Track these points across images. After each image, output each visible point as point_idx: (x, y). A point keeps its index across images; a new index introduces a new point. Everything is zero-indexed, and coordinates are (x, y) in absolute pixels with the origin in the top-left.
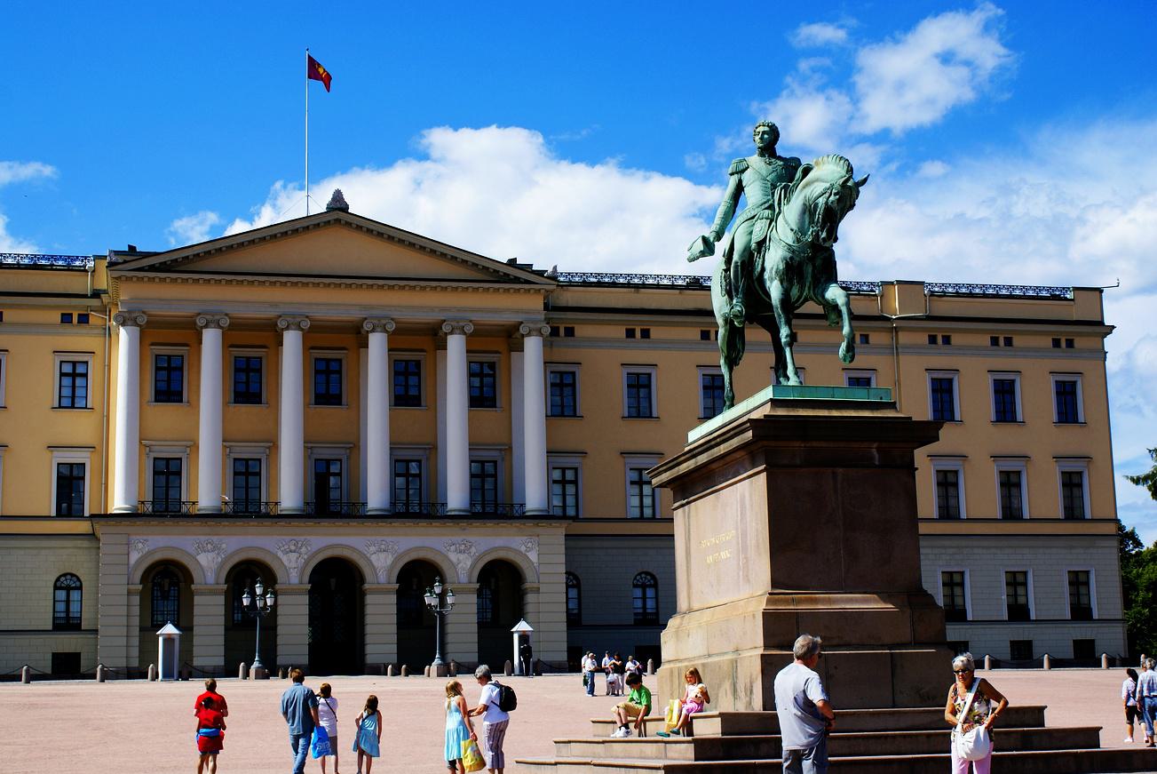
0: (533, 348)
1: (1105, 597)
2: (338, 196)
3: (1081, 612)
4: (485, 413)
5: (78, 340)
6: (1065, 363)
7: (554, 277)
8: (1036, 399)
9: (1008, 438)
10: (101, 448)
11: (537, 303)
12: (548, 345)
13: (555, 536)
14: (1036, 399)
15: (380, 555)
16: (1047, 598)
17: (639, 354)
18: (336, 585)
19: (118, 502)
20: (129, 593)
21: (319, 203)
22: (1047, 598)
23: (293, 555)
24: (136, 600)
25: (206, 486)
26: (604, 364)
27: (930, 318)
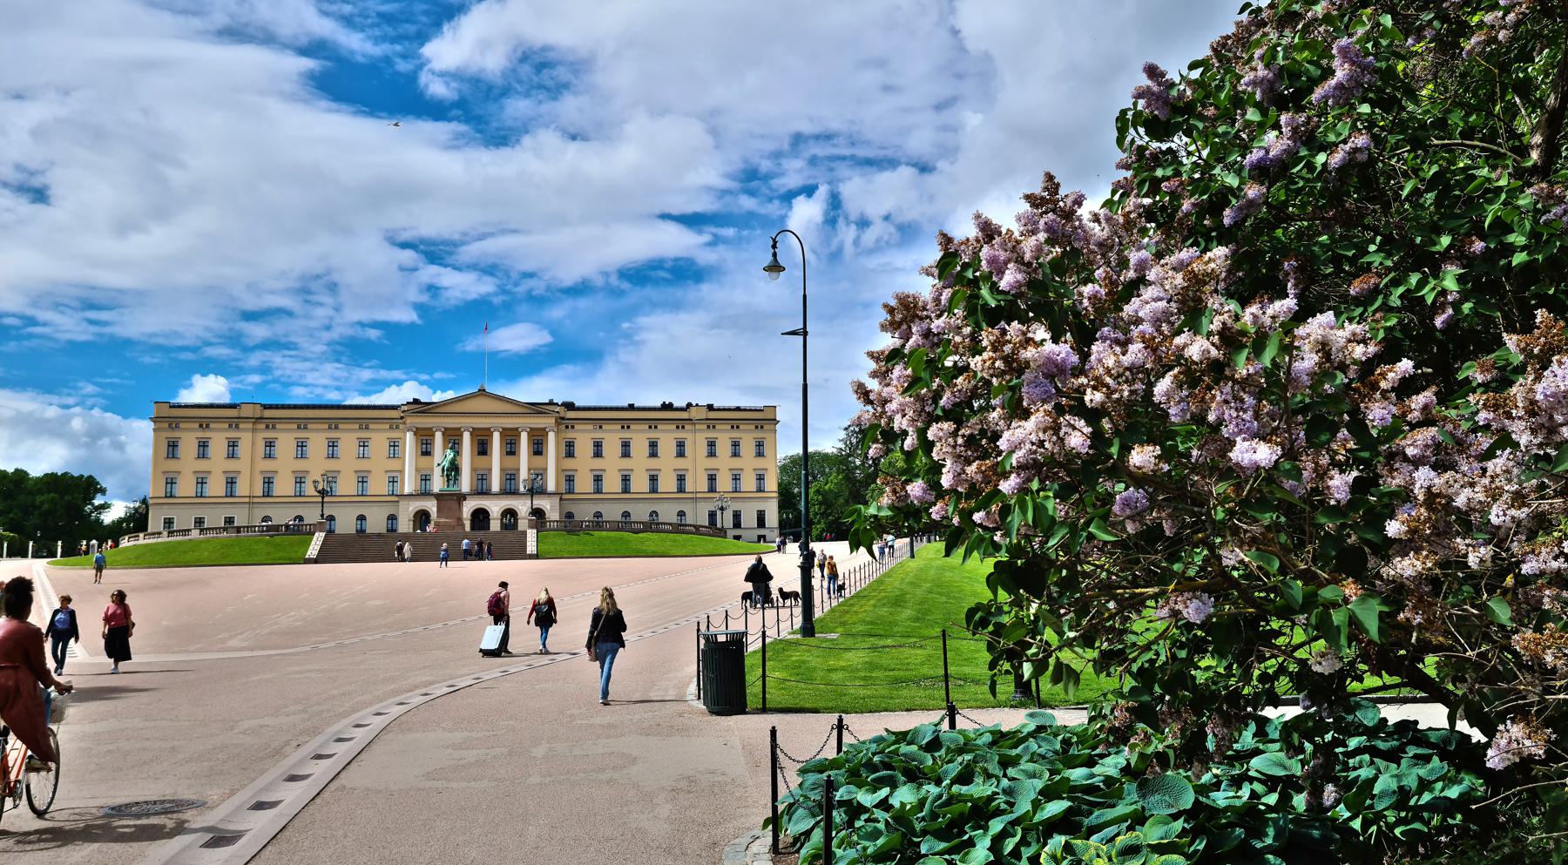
0: (551, 436)
1: (772, 519)
4: (538, 458)
5: (395, 434)
6: (759, 434)
7: (570, 406)
8: (748, 448)
10: (402, 472)
11: (553, 421)
12: (557, 433)
13: (556, 500)
14: (748, 448)
16: (749, 519)
17: (598, 435)
19: (407, 491)
22: (749, 519)
26: (584, 440)
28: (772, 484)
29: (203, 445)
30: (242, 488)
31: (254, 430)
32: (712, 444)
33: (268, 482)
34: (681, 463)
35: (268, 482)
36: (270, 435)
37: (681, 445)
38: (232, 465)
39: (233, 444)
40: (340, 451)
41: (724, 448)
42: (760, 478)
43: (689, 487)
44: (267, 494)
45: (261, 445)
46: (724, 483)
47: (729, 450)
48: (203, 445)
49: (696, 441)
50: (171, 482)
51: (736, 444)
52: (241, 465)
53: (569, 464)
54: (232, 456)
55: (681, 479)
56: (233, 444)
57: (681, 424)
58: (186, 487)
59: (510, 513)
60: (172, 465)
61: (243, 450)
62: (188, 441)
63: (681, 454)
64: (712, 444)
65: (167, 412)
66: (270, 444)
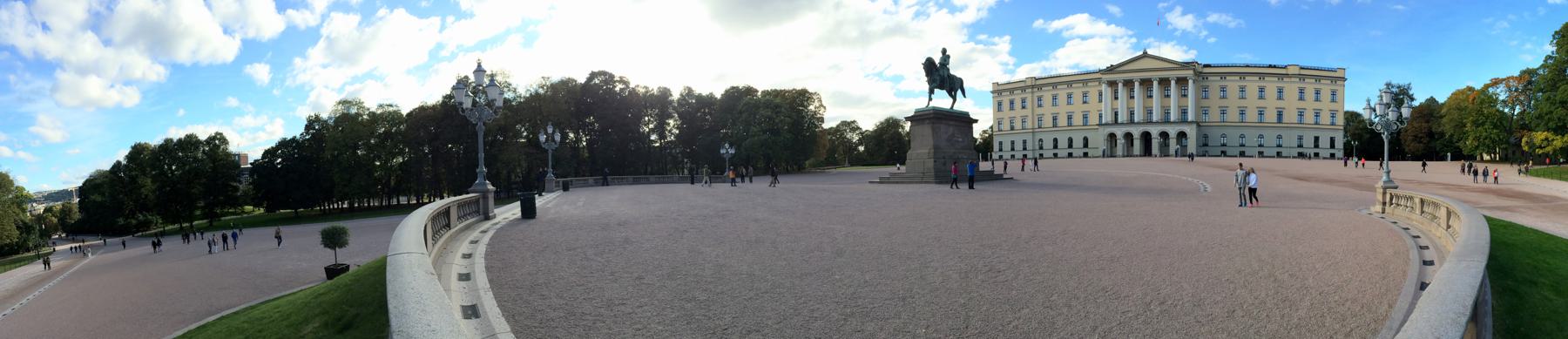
1: (1339, 144)
3: (1332, 146)
9: (1317, 105)
15: (1155, 131)
16: (1324, 143)
18: (1146, 137)
23: (1136, 132)
25: (1122, 118)
29: (1012, 103)
30: (1029, 125)
32: (1302, 91)
33: (1040, 120)
34: (1280, 104)
35: (1040, 120)
37: (1280, 91)
38: (1024, 112)
39: (1023, 101)
43: (1285, 119)
47: (1313, 96)
48: (1012, 103)
49: (1291, 88)
51: (1318, 92)
52: (1028, 112)
53: (1205, 103)
55: (1280, 115)
56: (1023, 101)
57: (1281, 76)
59: (1164, 135)
61: (1028, 104)
63: (1280, 98)
64: (1302, 91)
66: (1040, 99)
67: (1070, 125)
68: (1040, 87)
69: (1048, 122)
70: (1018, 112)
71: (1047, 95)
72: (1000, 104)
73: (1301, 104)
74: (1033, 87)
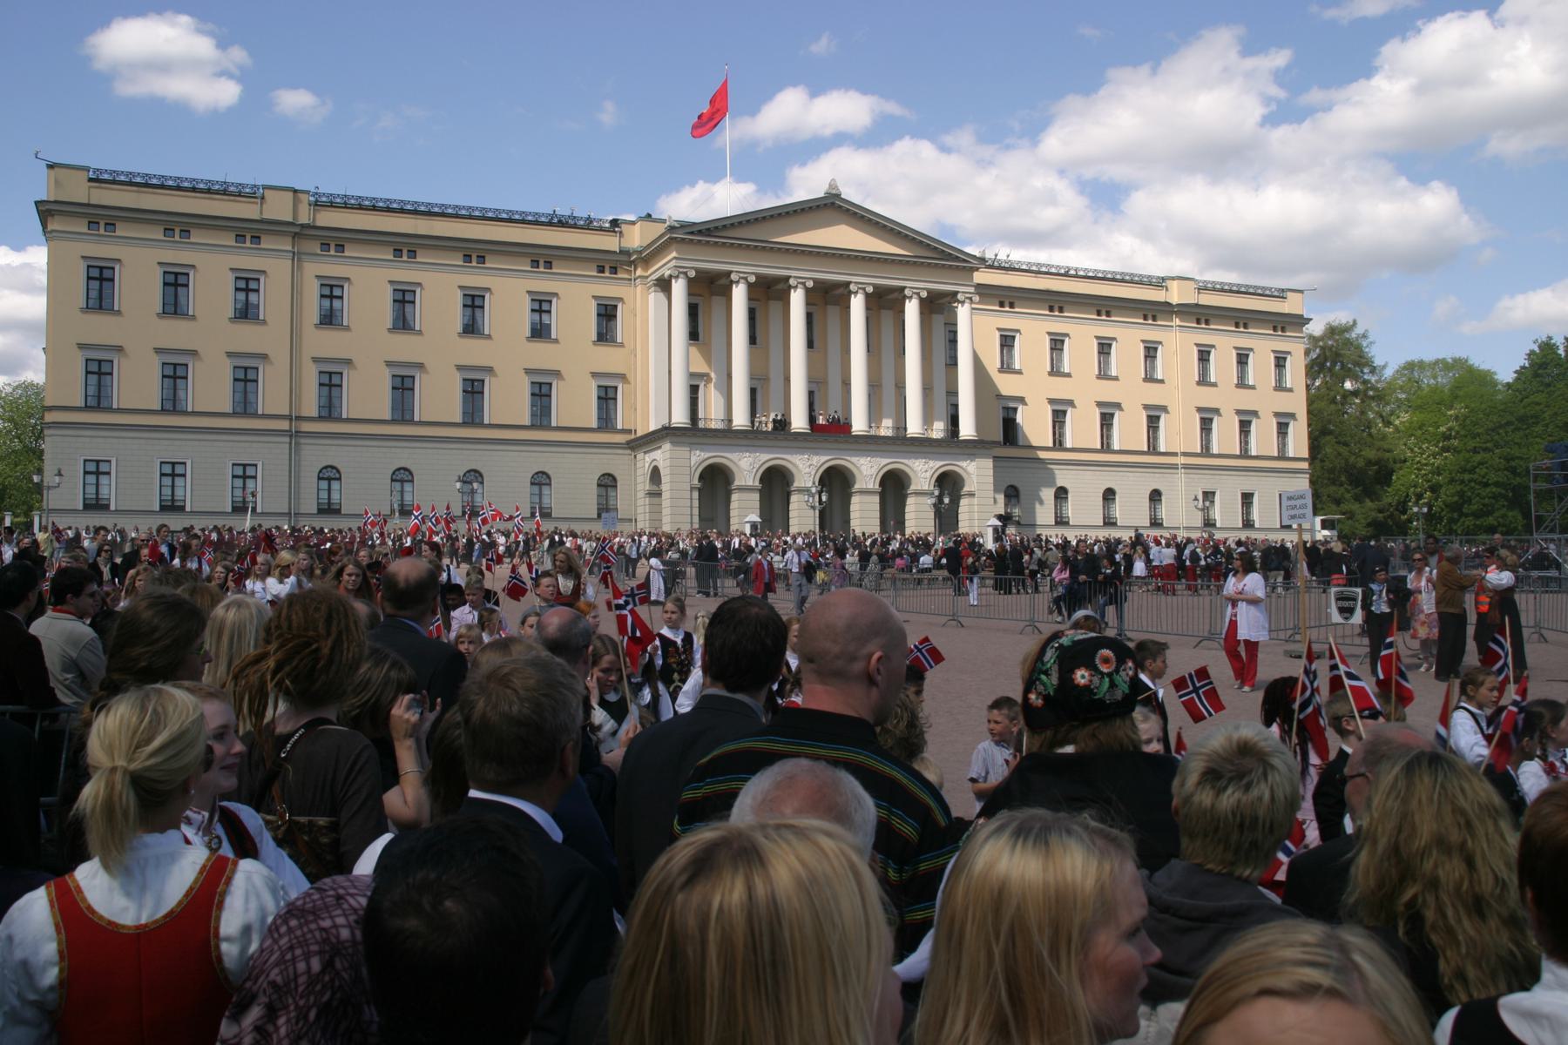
2: (833, 185)
20: (692, 489)
21: (818, 192)
24: (696, 494)
27: (1197, 305)
28: (1298, 442)
29: (175, 283)
30: (272, 395)
31: (297, 257)
33: (331, 383)
35: (331, 383)
36: (333, 269)
38: (247, 338)
39: (247, 284)
40: (491, 317)
41: (1223, 365)
42: (1282, 429)
44: (329, 411)
45: (312, 291)
46: (1225, 436)
48: (175, 283)
50: (99, 370)
54: (246, 313)
56: (247, 284)
58: (137, 384)
60: (101, 329)
61: (273, 298)
62: (140, 266)
65: (79, 191)
66: (332, 291)
67: (473, 416)
68: (336, 241)
69: (367, 395)
70: (210, 332)
71: (369, 285)
72: (101, 278)
73: (1207, 398)
74: (299, 232)
